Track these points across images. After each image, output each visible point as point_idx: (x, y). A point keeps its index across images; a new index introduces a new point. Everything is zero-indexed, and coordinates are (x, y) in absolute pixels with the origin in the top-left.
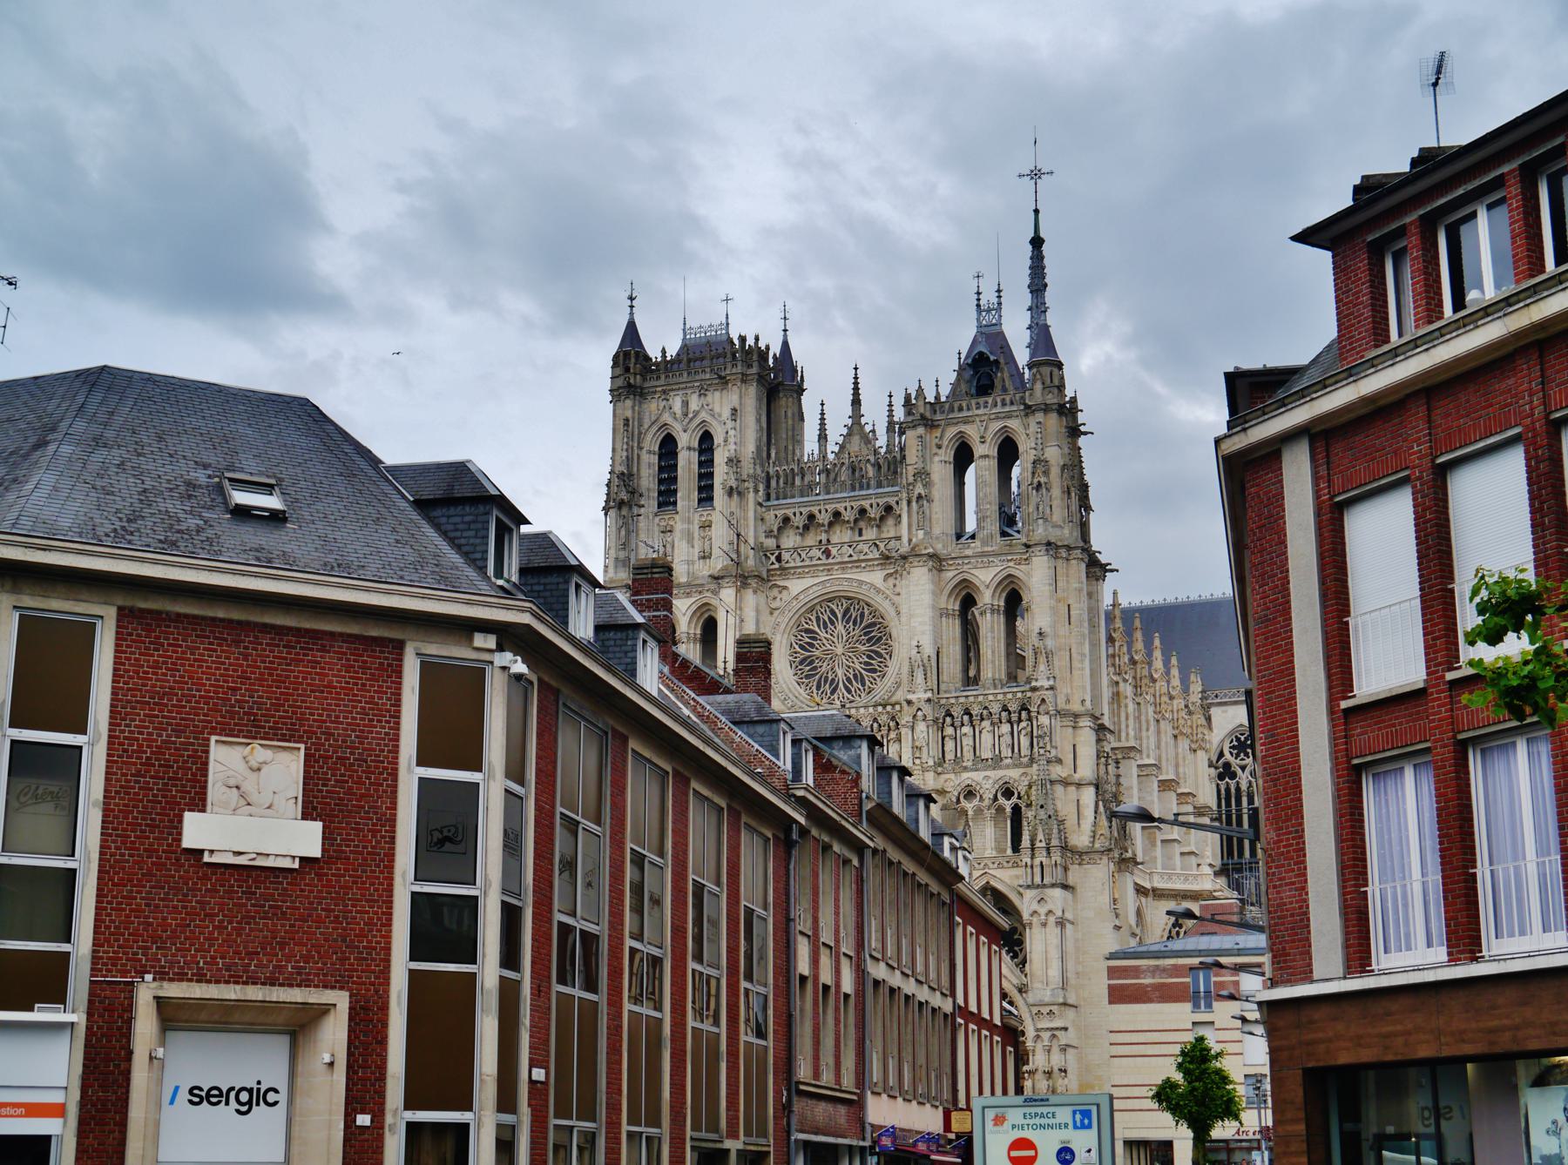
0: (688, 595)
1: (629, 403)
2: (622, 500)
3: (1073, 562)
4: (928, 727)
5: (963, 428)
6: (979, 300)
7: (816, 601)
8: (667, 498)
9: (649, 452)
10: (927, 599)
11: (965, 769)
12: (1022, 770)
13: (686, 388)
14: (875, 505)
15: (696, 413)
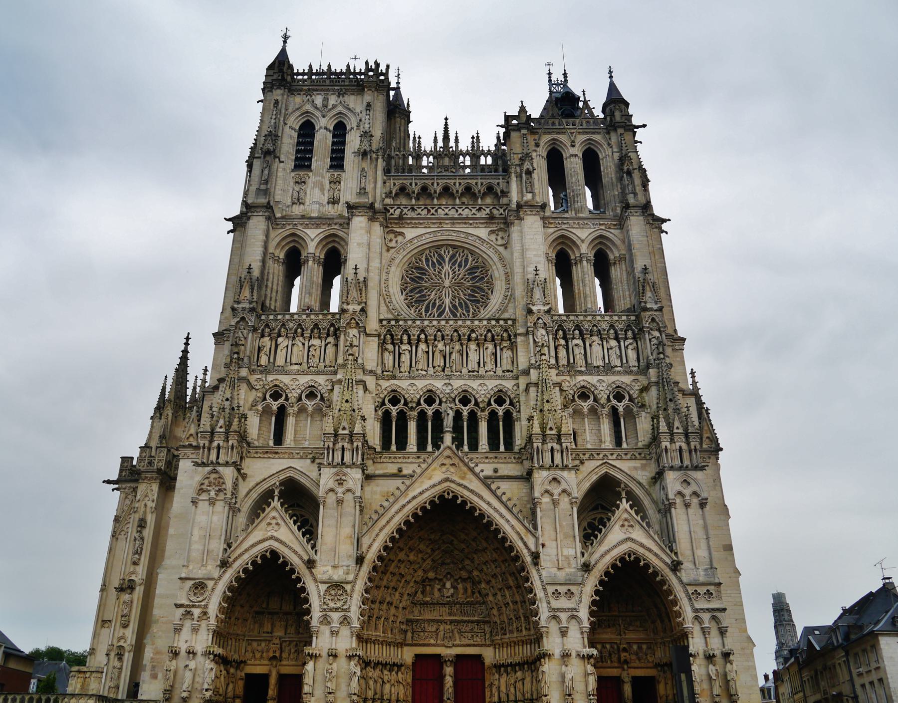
0: (318, 226)
1: (279, 92)
2: (269, 150)
3: (655, 230)
4: (547, 333)
5: (556, 136)
6: (550, 77)
7: (427, 246)
8: (303, 162)
9: (291, 128)
10: (540, 238)
11: (581, 373)
12: (633, 377)
13: (328, 90)
14: (479, 184)
15: (334, 107)
